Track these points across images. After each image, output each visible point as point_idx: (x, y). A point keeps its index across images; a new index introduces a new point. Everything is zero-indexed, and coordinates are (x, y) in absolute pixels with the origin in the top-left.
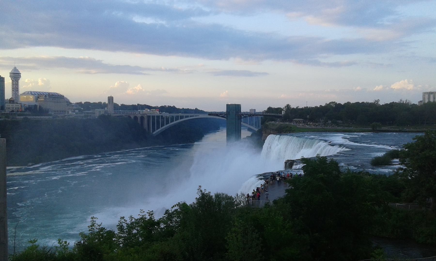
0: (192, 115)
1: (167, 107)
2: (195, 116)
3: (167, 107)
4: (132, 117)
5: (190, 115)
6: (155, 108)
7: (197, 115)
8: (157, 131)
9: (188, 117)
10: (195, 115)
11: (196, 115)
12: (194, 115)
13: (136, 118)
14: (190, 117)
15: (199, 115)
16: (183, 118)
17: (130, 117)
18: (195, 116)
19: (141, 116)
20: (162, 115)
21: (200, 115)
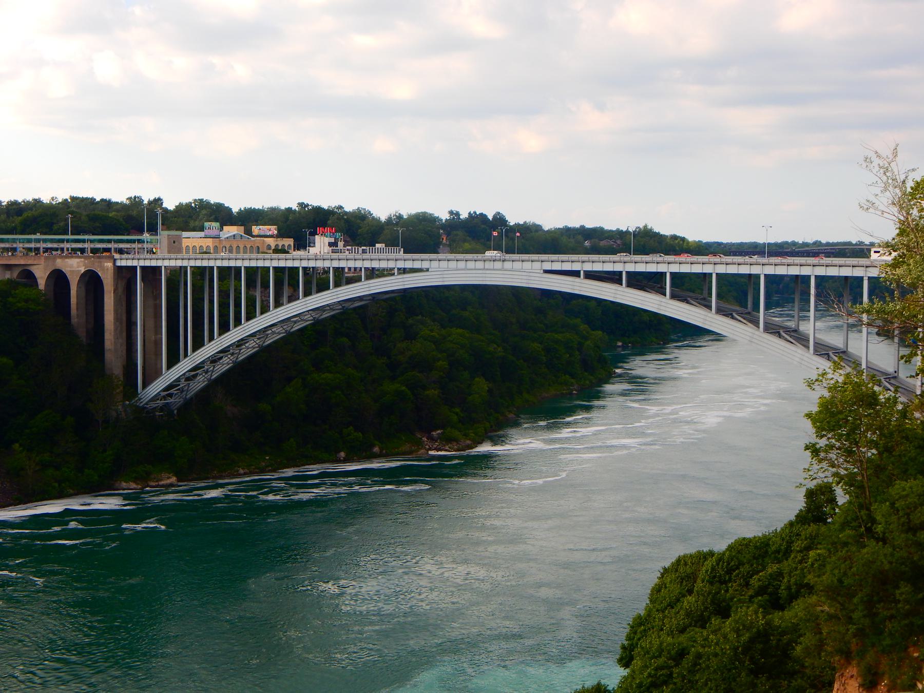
0: (383, 265)
1: (69, 200)
2: (404, 271)
3: (69, 200)
4: (41, 274)
5: (367, 264)
6: (249, 218)
7: (417, 265)
8: (170, 376)
9: (358, 279)
10: (401, 265)
11: (409, 265)
12: (391, 264)
13: (59, 278)
14: (368, 278)
15: (425, 265)
16: (328, 288)
17: (28, 276)
18: (404, 271)
19: (83, 270)
20: (154, 263)
21: (435, 264)
